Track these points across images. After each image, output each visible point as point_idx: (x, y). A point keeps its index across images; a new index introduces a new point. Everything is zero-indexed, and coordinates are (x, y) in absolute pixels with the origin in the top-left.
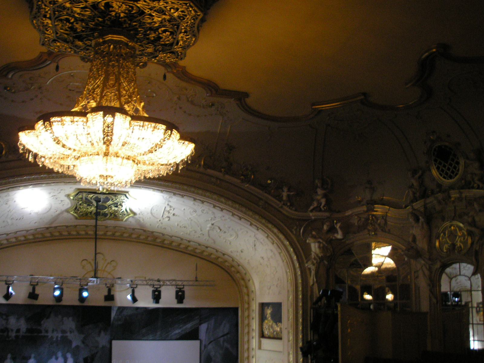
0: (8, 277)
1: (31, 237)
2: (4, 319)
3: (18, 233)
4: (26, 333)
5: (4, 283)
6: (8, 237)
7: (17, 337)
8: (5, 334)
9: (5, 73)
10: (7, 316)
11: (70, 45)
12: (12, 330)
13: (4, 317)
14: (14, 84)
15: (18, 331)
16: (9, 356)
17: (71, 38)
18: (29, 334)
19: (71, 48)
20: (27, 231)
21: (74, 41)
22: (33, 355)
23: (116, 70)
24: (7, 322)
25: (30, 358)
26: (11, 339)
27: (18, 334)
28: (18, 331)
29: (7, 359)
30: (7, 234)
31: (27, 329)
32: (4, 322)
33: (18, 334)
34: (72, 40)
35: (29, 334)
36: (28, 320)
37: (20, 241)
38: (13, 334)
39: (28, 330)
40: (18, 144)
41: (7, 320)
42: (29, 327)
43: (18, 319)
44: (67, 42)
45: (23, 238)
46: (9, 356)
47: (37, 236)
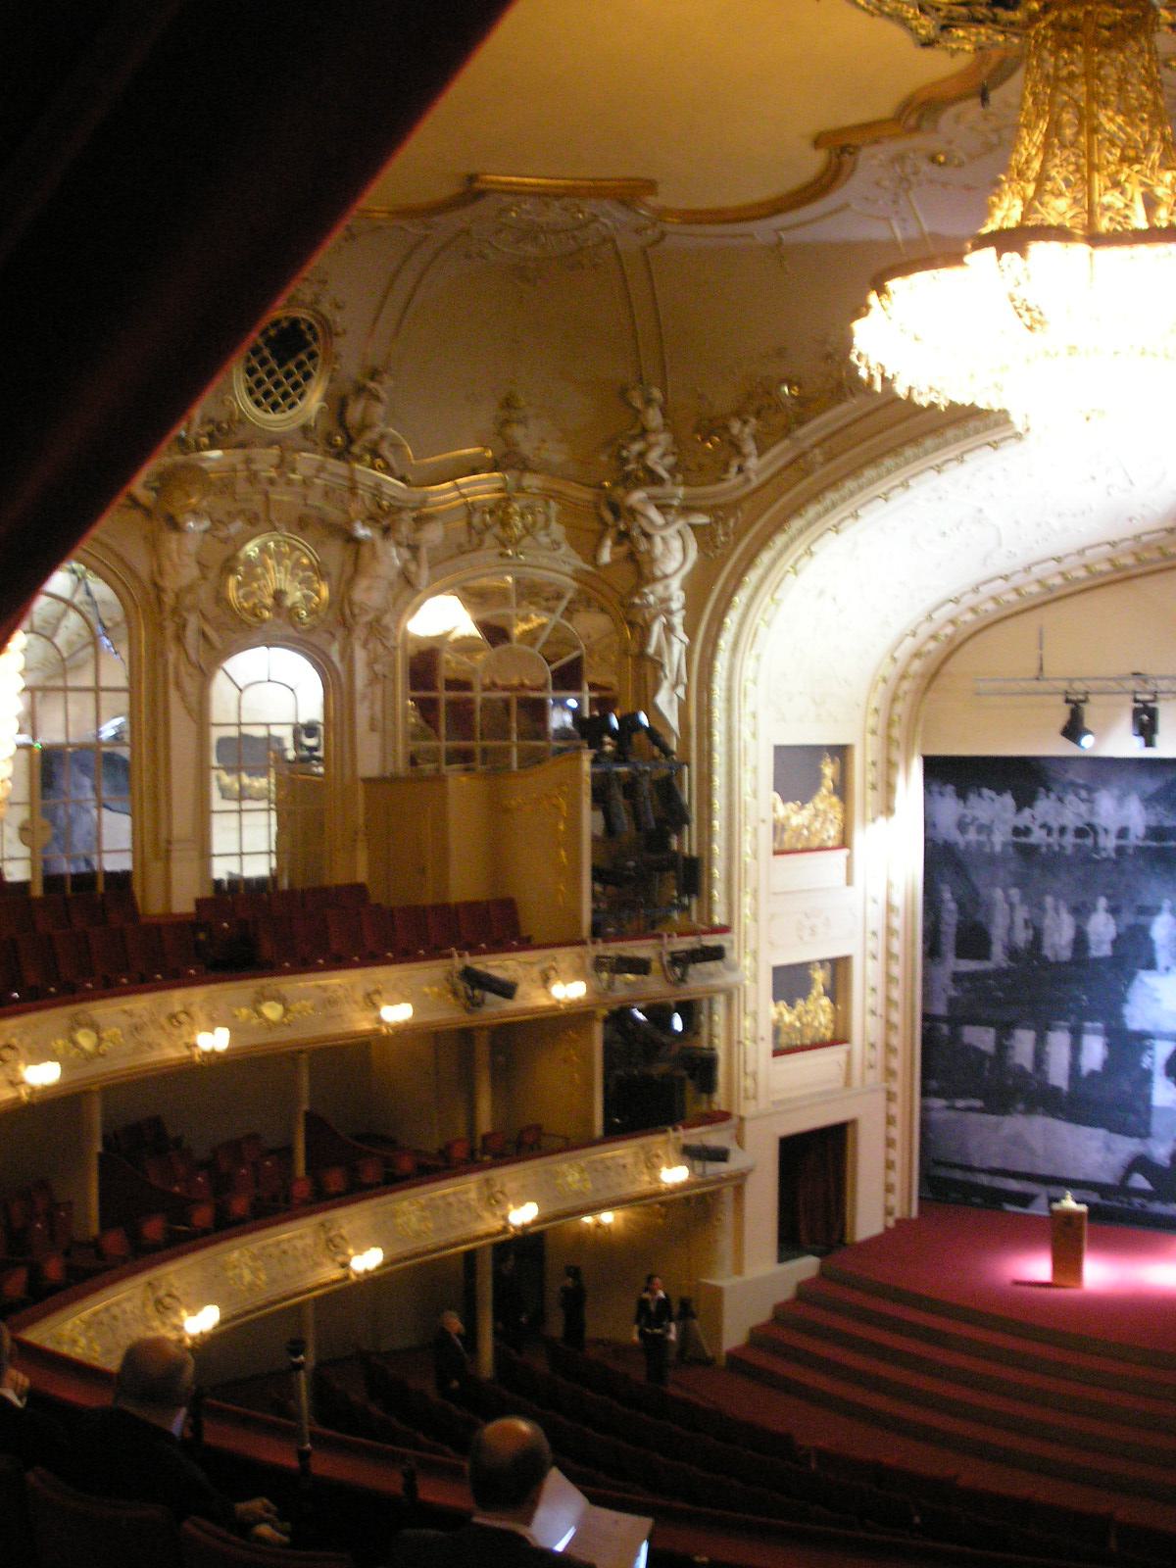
0: (1071, 680)
1: (1129, 561)
2: (1082, 800)
3: (1088, 553)
4: (1147, 837)
5: (1060, 699)
6: (1063, 567)
7: (1120, 850)
8: (1089, 842)
9: (912, 122)
10: (1090, 790)
11: (990, 24)
12: (1106, 831)
13: (1083, 794)
14: (950, 142)
15: (1123, 833)
16: (1102, 902)
17: (984, 11)
18: (1154, 844)
19: (1003, 32)
20: (1113, 544)
21: (995, 15)
22: (1167, 904)
23: (1081, 89)
24: (1093, 808)
25: (1155, 910)
26: (1104, 855)
27: (1122, 842)
28: (1123, 833)
29: (1094, 909)
30: (1058, 560)
31: (1148, 828)
32: (1083, 808)
33: (1122, 842)
34: (990, 15)
35: (1154, 844)
36: (1148, 801)
37: (1101, 573)
38: (1109, 843)
39: (1156, 833)
40: (853, 358)
41: (1090, 801)
42: (1153, 823)
43: (1121, 800)
44: (981, 22)
45: (1105, 567)
46: (1102, 902)
47: (1146, 555)
